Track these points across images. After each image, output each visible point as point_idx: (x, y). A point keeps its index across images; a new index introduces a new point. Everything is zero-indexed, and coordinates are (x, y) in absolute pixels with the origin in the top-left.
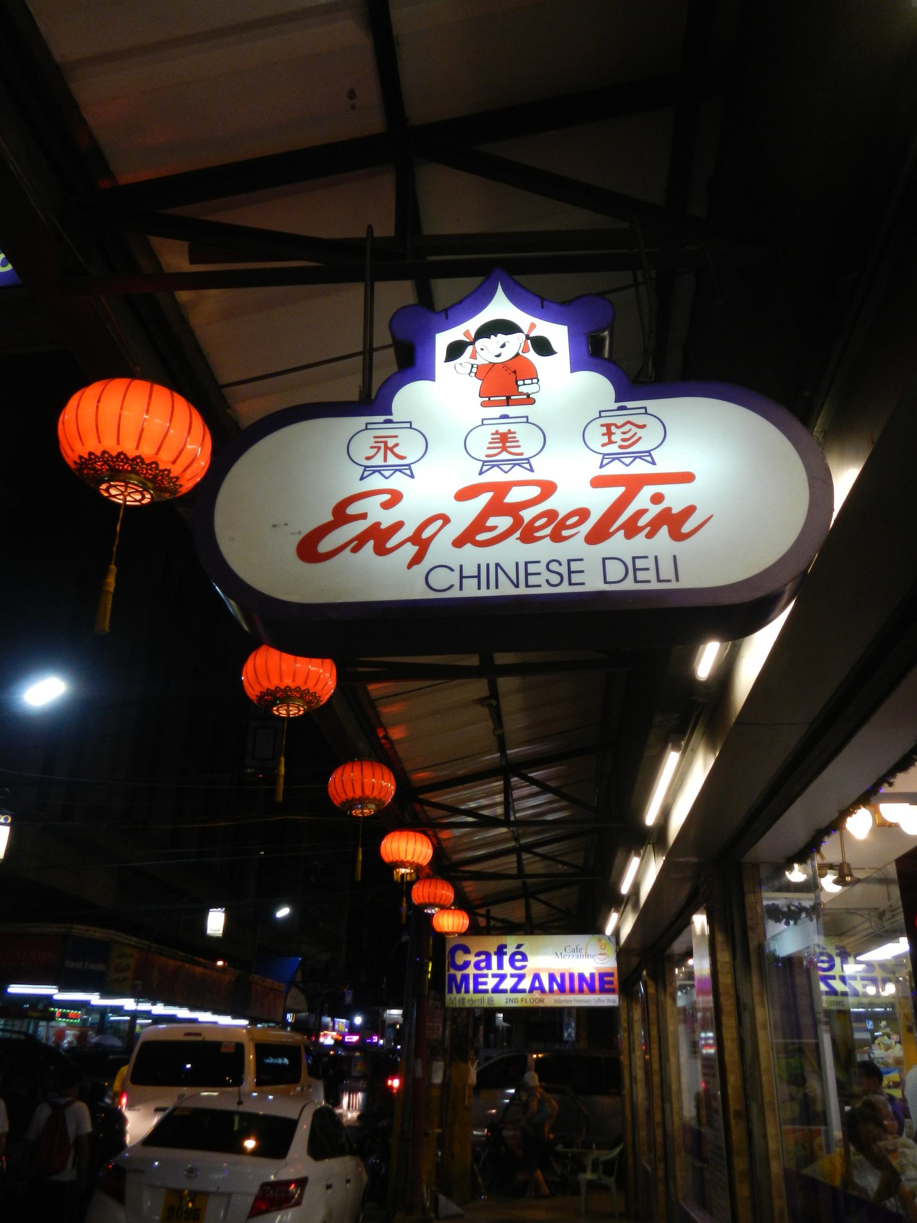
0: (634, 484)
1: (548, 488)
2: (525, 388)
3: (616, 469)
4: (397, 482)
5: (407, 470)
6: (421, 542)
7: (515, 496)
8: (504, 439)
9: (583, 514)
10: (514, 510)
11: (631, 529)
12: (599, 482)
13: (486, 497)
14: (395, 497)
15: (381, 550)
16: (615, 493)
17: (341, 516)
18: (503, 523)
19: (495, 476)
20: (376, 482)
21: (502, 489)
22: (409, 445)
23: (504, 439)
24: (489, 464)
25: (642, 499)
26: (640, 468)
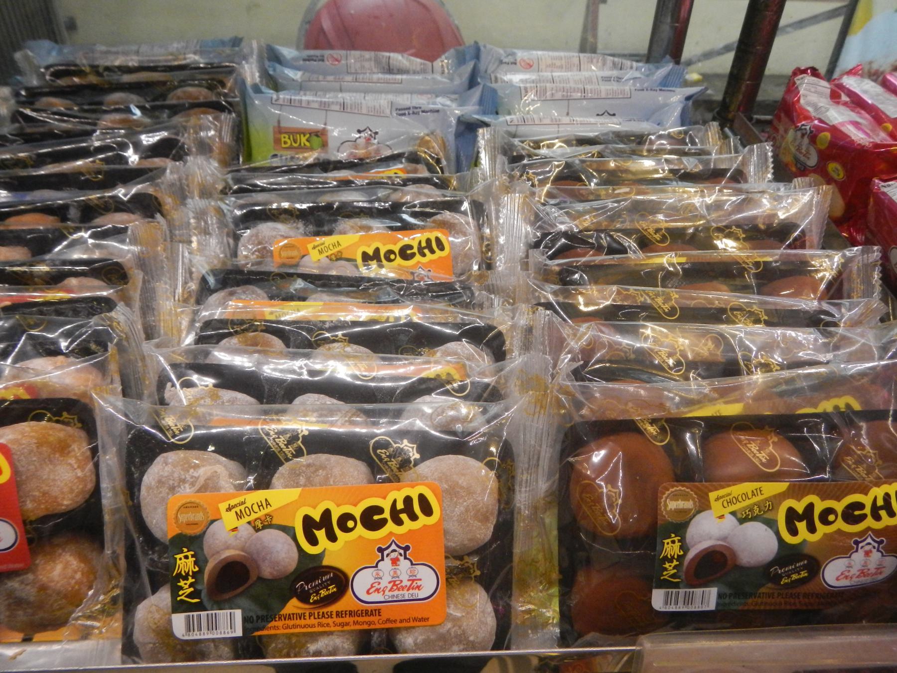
0: (413, 581)
1: (401, 581)
2: (398, 563)
3: (411, 578)
4: (380, 580)
5: (381, 578)
6: (384, 591)
7: (397, 583)
8: (395, 572)
9: (406, 586)
10: (396, 585)
11: (413, 589)
12: (409, 580)
13: (392, 584)
14: (379, 583)
15: (378, 593)
16: (410, 582)
17: (372, 587)
18: (395, 588)
19: (394, 579)
20: (377, 580)
21: (395, 582)
22: (381, 574)
23: (395, 572)
24: (393, 577)
25: (414, 584)
26: (414, 578)
